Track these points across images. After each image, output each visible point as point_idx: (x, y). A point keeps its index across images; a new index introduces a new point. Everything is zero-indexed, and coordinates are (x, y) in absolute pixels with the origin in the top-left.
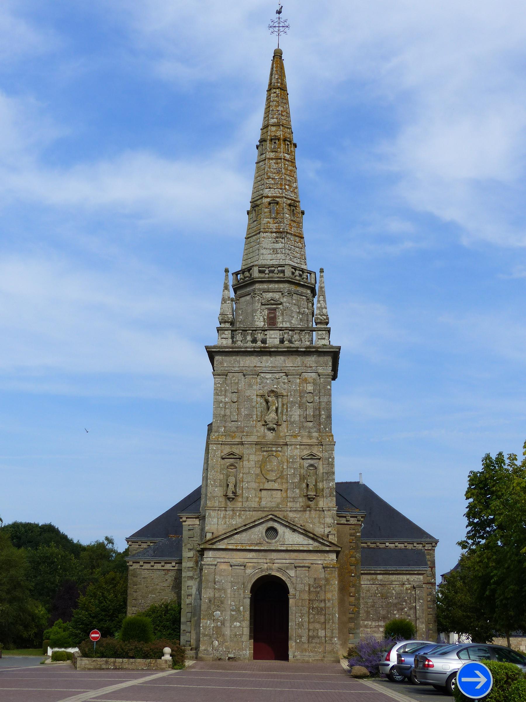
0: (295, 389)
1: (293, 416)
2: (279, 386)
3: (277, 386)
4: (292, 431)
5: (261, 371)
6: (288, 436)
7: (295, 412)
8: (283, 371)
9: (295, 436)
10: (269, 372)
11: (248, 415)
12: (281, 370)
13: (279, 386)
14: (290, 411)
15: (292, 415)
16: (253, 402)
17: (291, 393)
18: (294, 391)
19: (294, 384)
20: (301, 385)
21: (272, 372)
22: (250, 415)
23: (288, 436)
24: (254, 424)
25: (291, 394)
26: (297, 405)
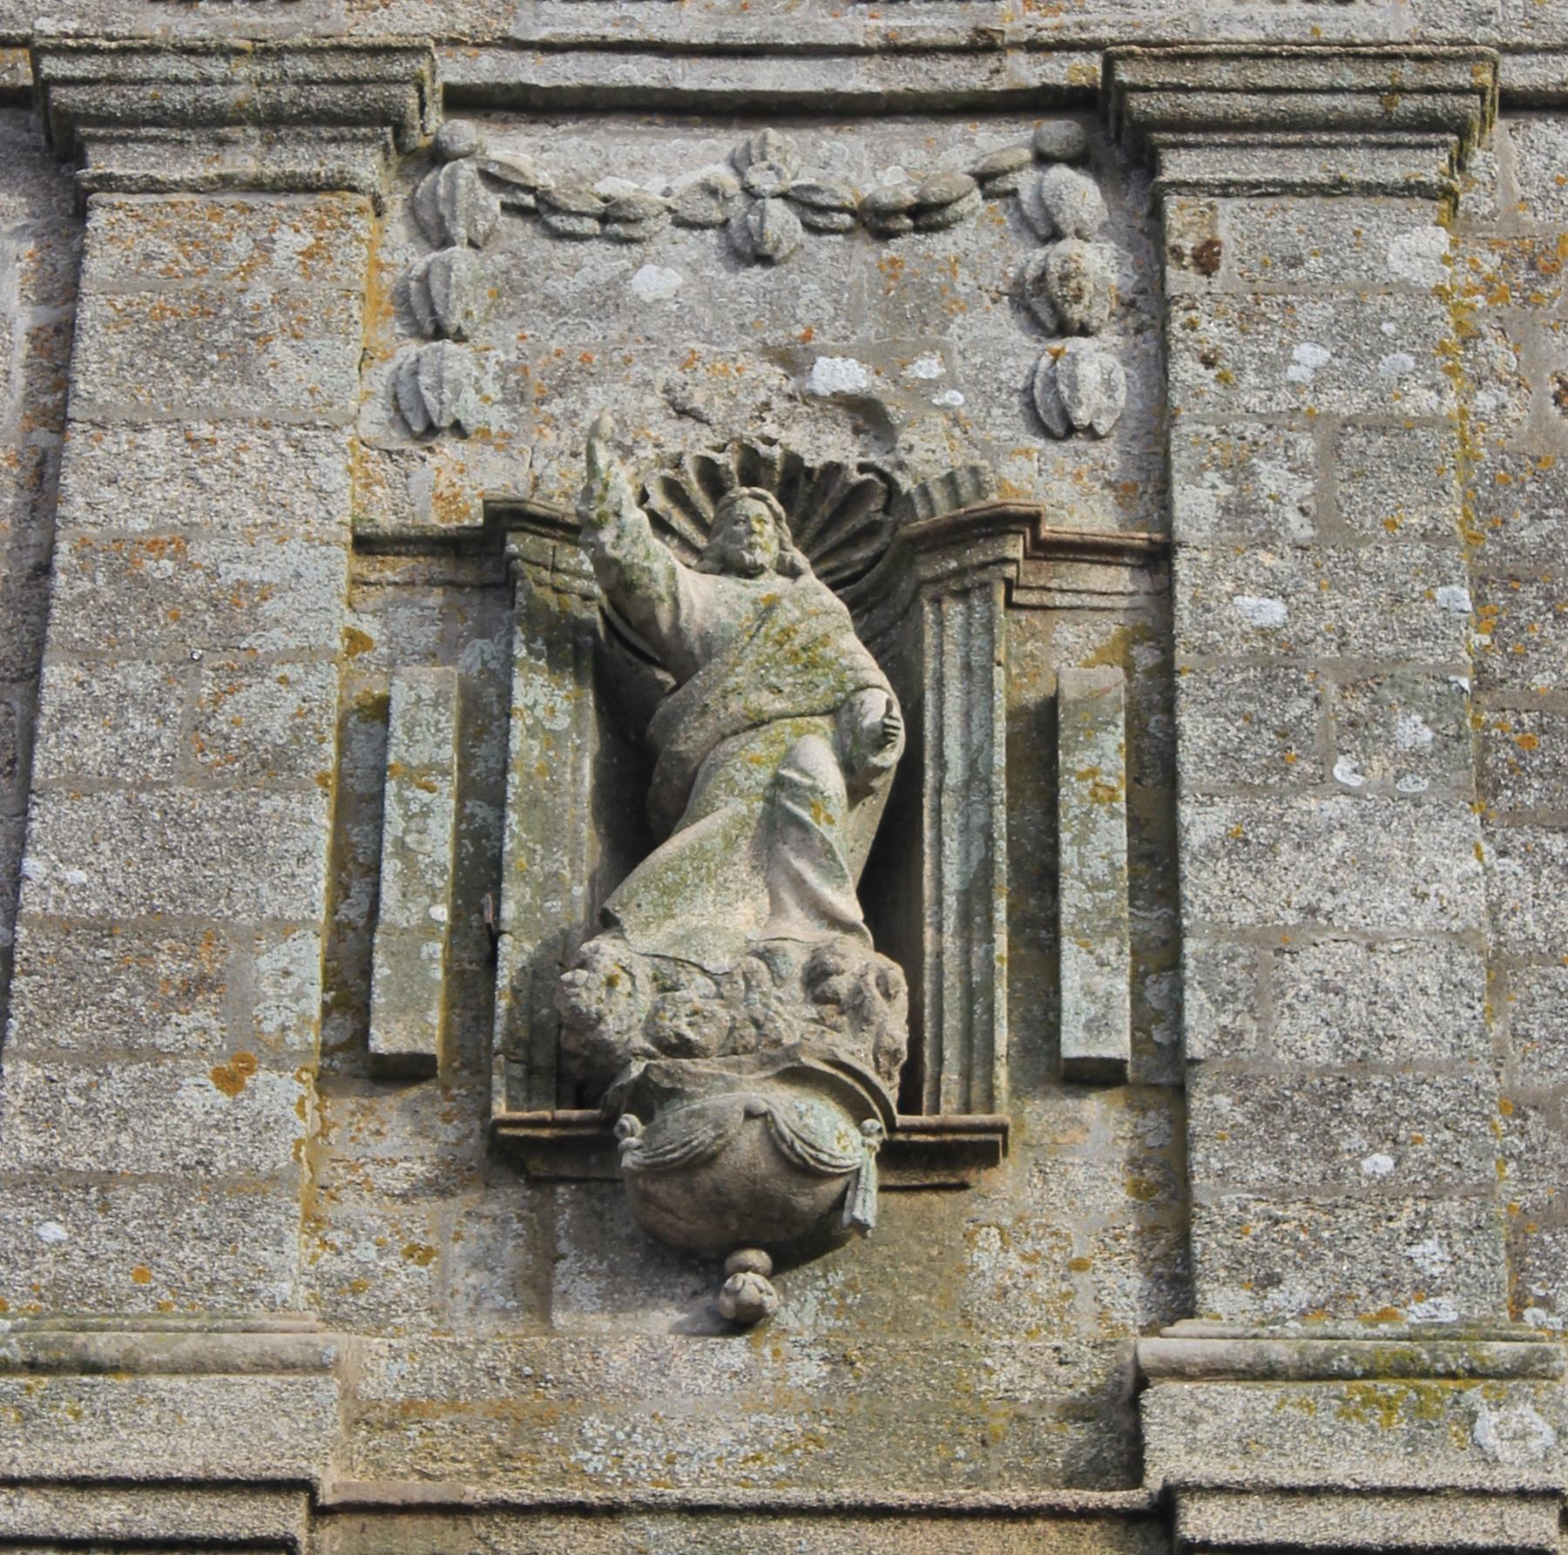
0: (1341, 402)
1: (1302, 970)
2: (927, 368)
3: (884, 357)
4: (1296, 1291)
5: (485, 69)
6: (1214, 1372)
7: (1368, 866)
8: (1026, 72)
9: (1404, 1370)
10: (691, 77)
11: (104, 929)
12: (983, 45)
13: (927, 368)
14: (1236, 842)
15: (1281, 943)
16: (255, 667)
17: (1239, 470)
18: (1333, 449)
19: (1317, 313)
20: (1499, 352)
21: (767, 77)
22: (154, 926)
23: (1214, 1372)
24: (262, 1128)
25: (1237, 511)
26: (1413, 731)
